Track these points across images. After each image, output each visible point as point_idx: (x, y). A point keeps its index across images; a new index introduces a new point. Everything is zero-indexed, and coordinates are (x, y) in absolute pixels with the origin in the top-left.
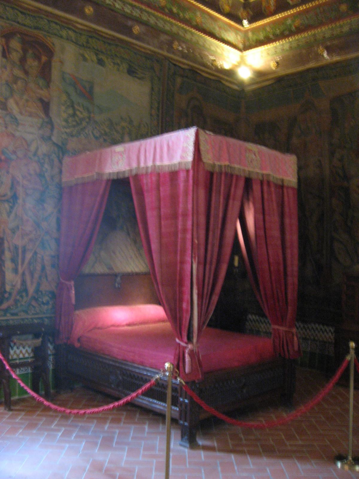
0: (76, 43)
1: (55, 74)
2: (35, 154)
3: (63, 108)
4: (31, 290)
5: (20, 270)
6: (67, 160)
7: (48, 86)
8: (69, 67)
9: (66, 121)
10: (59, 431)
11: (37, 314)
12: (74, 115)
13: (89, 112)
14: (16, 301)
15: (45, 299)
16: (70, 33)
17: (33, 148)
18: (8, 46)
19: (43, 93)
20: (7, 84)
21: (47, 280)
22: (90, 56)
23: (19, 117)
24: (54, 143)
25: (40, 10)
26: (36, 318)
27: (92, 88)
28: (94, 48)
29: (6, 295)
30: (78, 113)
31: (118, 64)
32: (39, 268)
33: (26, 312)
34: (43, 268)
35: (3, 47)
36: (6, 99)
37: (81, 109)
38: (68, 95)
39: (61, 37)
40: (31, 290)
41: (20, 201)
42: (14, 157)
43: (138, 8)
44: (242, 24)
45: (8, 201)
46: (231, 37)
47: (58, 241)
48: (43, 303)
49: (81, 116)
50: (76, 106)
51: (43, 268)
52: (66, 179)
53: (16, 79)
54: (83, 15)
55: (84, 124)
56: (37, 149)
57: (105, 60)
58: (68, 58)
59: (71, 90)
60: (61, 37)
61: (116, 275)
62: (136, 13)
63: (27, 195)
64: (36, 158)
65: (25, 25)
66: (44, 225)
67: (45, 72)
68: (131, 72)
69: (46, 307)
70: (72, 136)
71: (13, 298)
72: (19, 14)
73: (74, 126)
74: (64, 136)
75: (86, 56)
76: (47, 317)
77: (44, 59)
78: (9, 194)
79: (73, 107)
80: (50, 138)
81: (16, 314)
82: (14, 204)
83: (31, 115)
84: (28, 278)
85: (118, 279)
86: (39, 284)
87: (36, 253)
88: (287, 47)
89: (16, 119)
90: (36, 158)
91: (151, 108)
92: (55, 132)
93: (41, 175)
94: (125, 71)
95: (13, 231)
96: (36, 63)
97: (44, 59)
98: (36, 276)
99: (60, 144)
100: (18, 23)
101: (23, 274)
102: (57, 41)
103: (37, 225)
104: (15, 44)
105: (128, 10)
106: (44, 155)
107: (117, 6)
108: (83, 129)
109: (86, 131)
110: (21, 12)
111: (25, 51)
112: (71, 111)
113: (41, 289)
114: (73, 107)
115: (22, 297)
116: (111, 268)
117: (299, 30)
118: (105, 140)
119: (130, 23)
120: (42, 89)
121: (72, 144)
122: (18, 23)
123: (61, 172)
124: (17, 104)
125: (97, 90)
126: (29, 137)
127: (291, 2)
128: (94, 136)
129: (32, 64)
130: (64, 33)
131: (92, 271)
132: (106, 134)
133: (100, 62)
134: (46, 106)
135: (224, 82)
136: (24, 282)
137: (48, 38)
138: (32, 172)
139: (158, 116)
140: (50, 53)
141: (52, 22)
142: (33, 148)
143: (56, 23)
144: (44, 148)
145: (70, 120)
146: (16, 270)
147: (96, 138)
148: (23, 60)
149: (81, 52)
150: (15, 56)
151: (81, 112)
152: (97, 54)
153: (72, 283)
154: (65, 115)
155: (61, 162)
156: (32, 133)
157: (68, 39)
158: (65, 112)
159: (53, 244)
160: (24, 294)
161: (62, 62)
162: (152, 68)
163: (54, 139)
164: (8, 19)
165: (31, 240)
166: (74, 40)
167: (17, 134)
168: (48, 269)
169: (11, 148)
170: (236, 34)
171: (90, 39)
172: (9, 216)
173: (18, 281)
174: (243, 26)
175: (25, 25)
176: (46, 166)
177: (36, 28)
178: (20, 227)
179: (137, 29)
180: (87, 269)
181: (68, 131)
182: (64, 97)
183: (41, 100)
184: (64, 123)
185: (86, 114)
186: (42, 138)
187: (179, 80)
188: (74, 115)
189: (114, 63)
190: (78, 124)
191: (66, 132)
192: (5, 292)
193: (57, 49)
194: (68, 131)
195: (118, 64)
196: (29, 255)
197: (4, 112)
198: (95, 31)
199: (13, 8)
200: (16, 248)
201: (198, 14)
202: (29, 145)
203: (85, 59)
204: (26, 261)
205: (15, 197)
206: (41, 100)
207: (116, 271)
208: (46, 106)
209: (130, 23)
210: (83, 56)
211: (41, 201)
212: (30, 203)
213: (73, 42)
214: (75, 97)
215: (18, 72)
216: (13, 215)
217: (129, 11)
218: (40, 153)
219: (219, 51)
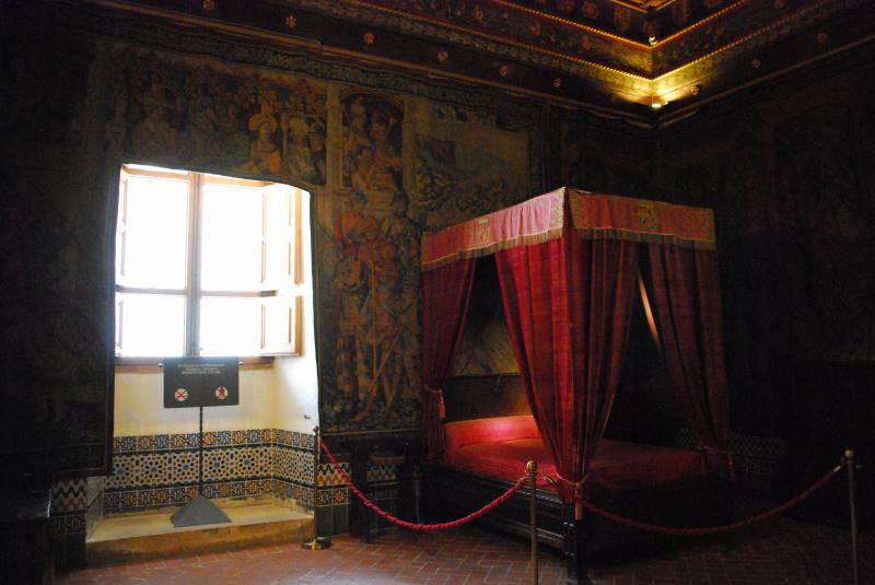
1: (407, 136)
2: (387, 235)
3: (418, 177)
4: (390, 399)
5: (376, 375)
6: (425, 239)
7: (399, 152)
8: (423, 129)
9: (423, 192)
10: (421, 565)
11: (399, 427)
12: (433, 183)
13: (451, 179)
14: (372, 412)
15: (408, 409)
16: (422, 86)
17: (385, 228)
18: (349, 112)
19: (395, 162)
20: (350, 155)
21: (409, 386)
23: (365, 192)
24: (411, 221)
26: (398, 433)
29: (360, 405)
30: (437, 181)
32: (398, 370)
33: (385, 425)
34: (404, 370)
35: (344, 114)
36: (350, 173)
37: (440, 176)
38: (424, 161)
39: (411, 93)
40: (390, 399)
41: (372, 292)
42: (363, 240)
43: (504, 44)
45: (358, 292)
46: (635, 60)
47: (420, 338)
48: (407, 416)
49: (442, 185)
50: (434, 174)
51: (404, 370)
52: (429, 261)
53: (360, 149)
54: (436, 64)
55: (446, 193)
56: (390, 229)
57: (467, 113)
58: (420, 118)
60: (411, 93)
61: (495, 377)
62: (503, 51)
63: (379, 282)
64: (389, 240)
65: (366, 85)
66: (403, 319)
67: (394, 137)
68: (501, 124)
69: (408, 419)
70: (432, 210)
71: (368, 408)
72: (361, 73)
73: (433, 198)
75: (443, 110)
76: (410, 432)
77: (392, 121)
78: (360, 284)
80: (404, 215)
81: (373, 428)
82: (365, 296)
83: (380, 189)
84: (386, 384)
85: (499, 381)
86: (399, 392)
87: (393, 354)
88: (709, 64)
89: (363, 196)
90: (389, 240)
91: (531, 166)
92: (410, 205)
93: (396, 260)
95: (366, 328)
96: (383, 128)
97: (392, 121)
98: (396, 379)
99: (417, 220)
100: (359, 83)
101: (380, 379)
102: (406, 98)
103: (395, 320)
104: (358, 109)
106: (399, 235)
107: (477, 45)
108: (445, 200)
109: (449, 202)
110: (363, 71)
111: (369, 115)
112: (428, 181)
113: (403, 397)
114: (430, 174)
115: (379, 406)
116: (488, 369)
117: (723, 42)
118: (473, 212)
119: (496, 64)
121: (432, 220)
122: (359, 83)
123: (419, 254)
124: (364, 177)
126: (379, 215)
127: (709, 6)
128: (458, 205)
129: (377, 128)
130: (414, 88)
131: (465, 373)
132: (474, 204)
133: (461, 117)
134: (397, 176)
135: (628, 121)
136: (381, 390)
138: (385, 256)
139: (541, 175)
140: (399, 114)
142: (385, 228)
143: (403, 77)
144: (398, 227)
145: (428, 190)
146: (370, 375)
147: (461, 209)
148: (368, 124)
150: (358, 123)
151: (441, 180)
152: (456, 109)
153: (441, 391)
154: (421, 185)
155: (419, 241)
156: (384, 211)
157: (419, 94)
158: (421, 181)
159: (414, 341)
160: (381, 403)
164: (347, 80)
165: (386, 338)
167: (365, 212)
168: (410, 373)
169: (359, 230)
170: (642, 56)
172: (359, 310)
173: (374, 386)
174: (649, 44)
175: (366, 85)
176: (402, 248)
177: (381, 86)
178: (374, 323)
179: (504, 70)
180: (458, 371)
181: (426, 203)
182: (419, 165)
183: (391, 170)
184: (421, 196)
185: (447, 182)
186: (396, 215)
188: (433, 183)
189: (480, 117)
190: (438, 195)
192: (359, 401)
193: (406, 109)
194: (426, 203)
196: (385, 357)
197: (350, 189)
199: (353, 68)
200: (370, 347)
201: (585, 38)
202: (380, 226)
203: (442, 116)
204: (382, 365)
205: (366, 288)
207: (496, 372)
208: (397, 176)
209: (496, 64)
211: (397, 291)
212: (385, 293)
214: (431, 162)
215: (361, 140)
216: (364, 310)
217: (493, 50)
218: (393, 232)
219: (618, 82)
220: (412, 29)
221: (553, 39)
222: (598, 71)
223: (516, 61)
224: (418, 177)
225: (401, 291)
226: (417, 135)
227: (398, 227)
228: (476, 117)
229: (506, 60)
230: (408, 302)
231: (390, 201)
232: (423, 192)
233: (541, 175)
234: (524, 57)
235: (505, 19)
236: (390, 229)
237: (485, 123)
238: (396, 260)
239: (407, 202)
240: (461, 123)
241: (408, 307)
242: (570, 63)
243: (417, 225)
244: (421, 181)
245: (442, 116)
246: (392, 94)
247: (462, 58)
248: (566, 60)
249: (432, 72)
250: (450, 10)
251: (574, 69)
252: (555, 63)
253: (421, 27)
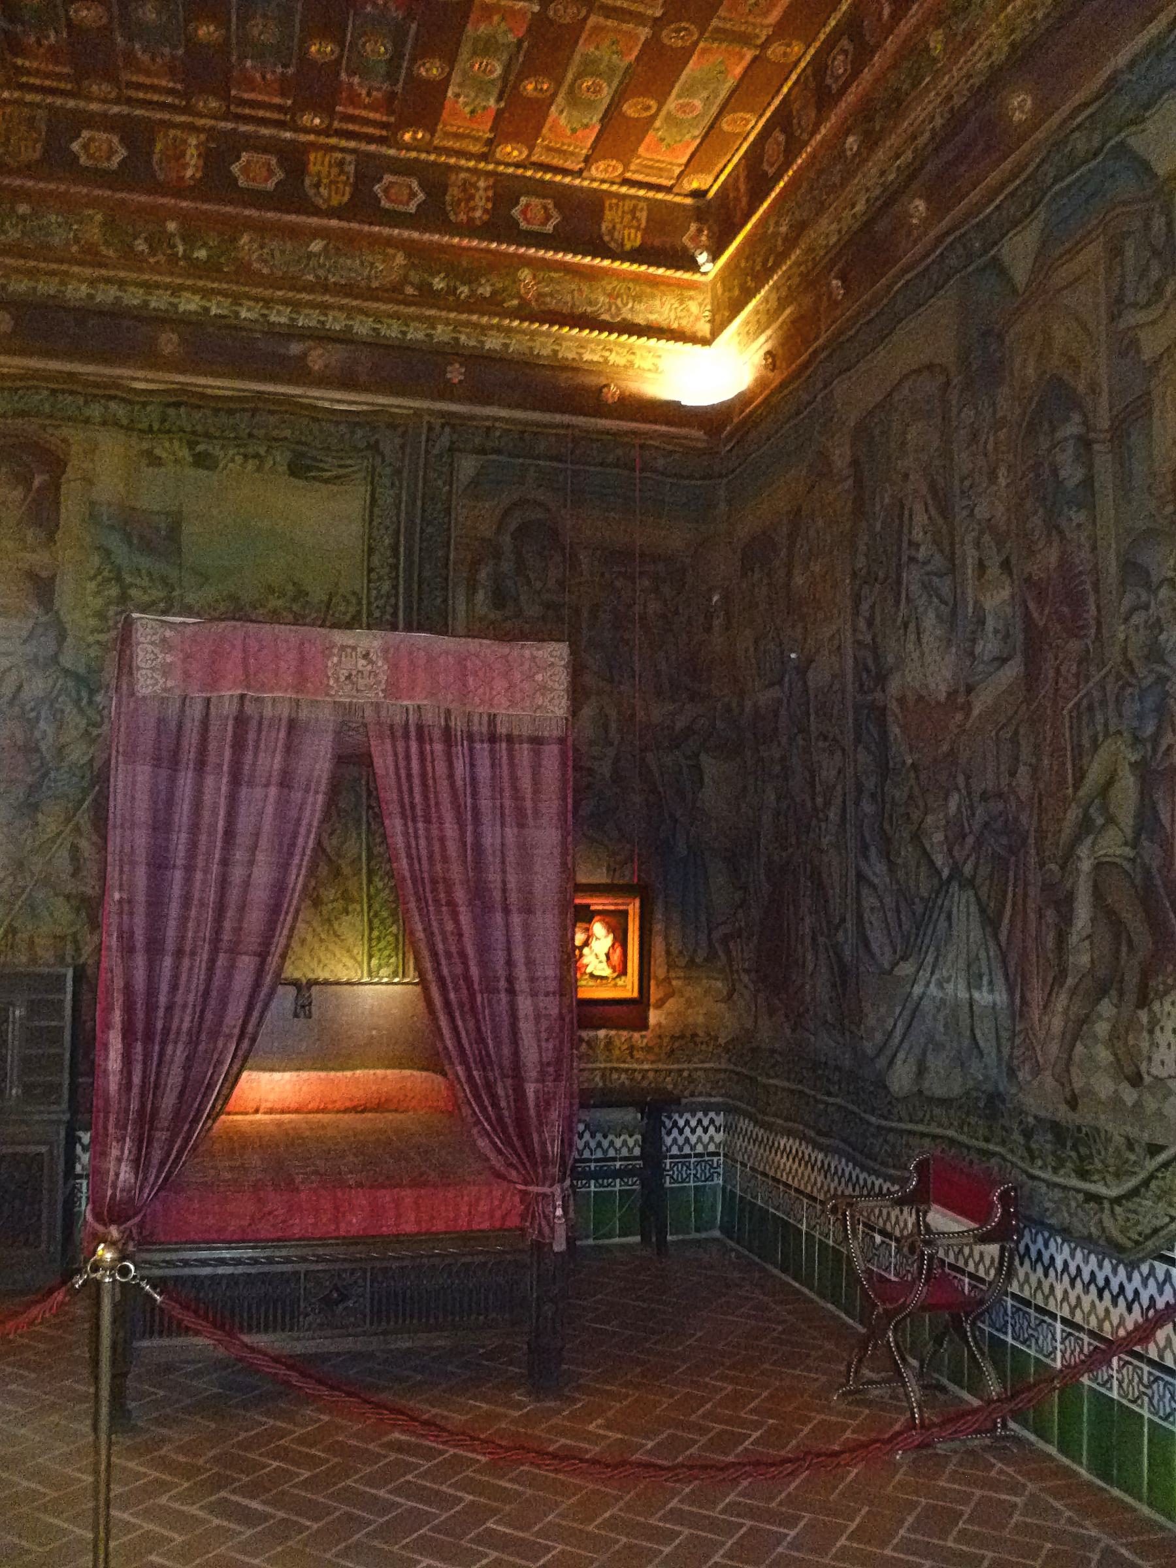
0: (128, 429)
1: (71, 509)
2: (11, 703)
3: (91, 586)
7: (51, 538)
9: (101, 615)
19: (38, 559)
22: (172, 449)
24: (67, 672)
25: (35, 375)
27: (174, 530)
28: (183, 430)
30: (133, 592)
31: (256, 456)
37: (145, 583)
44: (694, 266)
50: (128, 579)
56: (20, 688)
57: (218, 452)
58: (105, 467)
59: (114, 542)
60: (87, 421)
62: (307, 319)
66: (37, 864)
68: (299, 468)
74: (93, 652)
79: (119, 579)
80: (55, 659)
91: (371, 551)
94: (282, 468)
99: (82, 670)
105: (279, 317)
112: (114, 591)
119: (295, 348)
120: (34, 551)
125: (189, 529)
130: (95, 411)
133: (202, 461)
134: (42, 588)
137: (50, 430)
141: (63, 392)
145: (113, 610)
149: (145, 445)
151: (144, 590)
152: (191, 445)
154: (98, 603)
161: (89, 481)
162: (374, 447)
163: (67, 661)
166: (125, 422)
171: (171, 411)
176: (42, 725)
177: (22, 414)
179: (317, 359)
184: (93, 622)
187: (468, 466)
189: (245, 456)
191: (98, 642)
195: (256, 456)
198: (184, 390)
206: (31, 576)
208: (42, 588)
209: (295, 348)
210: (149, 453)
213: (122, 427)
218: (25, 695)
220: (91, 297)
221: (438, 284)
222: (558, 340)
223: (345, 338)
224: (91, 586)
225: (35, 807)
226: (93, 504)
227: (38, 686)
228: (239, 459)
229: (323, 337)
230: (52, 829)
231: (25, 634)
232: (101, 615)
233: (395, 567)
234: (362, 327)
235: (310, 256)
236: (20, 688)
237: (259, 469)
238: (30, 749)
239: (62, 637)
240: (202, 473)
241: (53, 840)
242: (484, 329)
243: (78, 678)
244: (97, 593)
245: (155, 461)
246: (44, 428)
247: (212, 344)
248: (468, 323)
249: (141, 379)
250: (180, 249)
251: (493, 343)
252: (442, 333)
253: (113, 291)
